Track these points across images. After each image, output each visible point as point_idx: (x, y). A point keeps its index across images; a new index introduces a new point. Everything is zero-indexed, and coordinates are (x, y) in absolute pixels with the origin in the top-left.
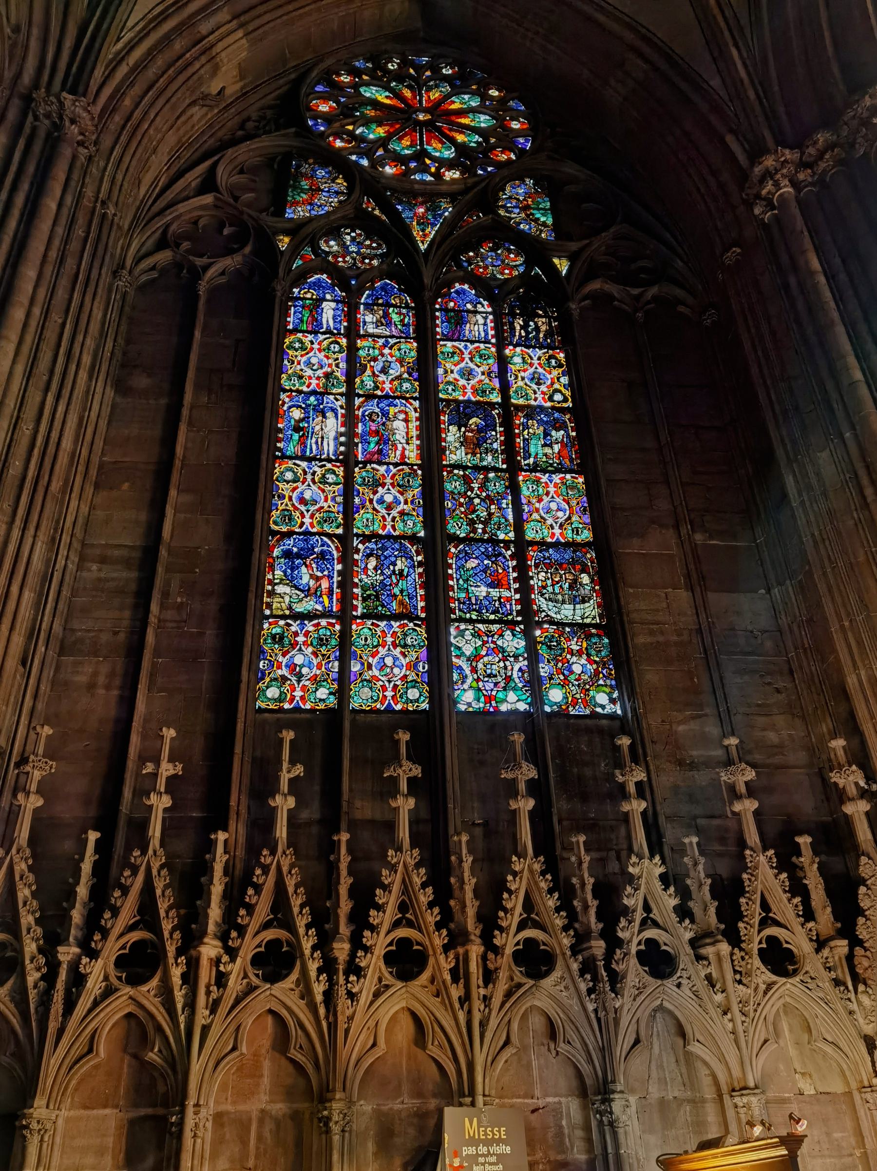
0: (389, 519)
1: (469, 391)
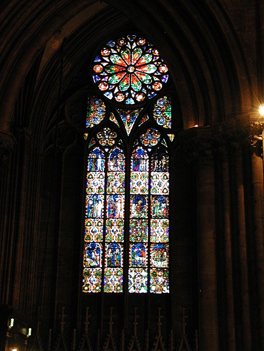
0: (115, 236)
1: (139, 190)
